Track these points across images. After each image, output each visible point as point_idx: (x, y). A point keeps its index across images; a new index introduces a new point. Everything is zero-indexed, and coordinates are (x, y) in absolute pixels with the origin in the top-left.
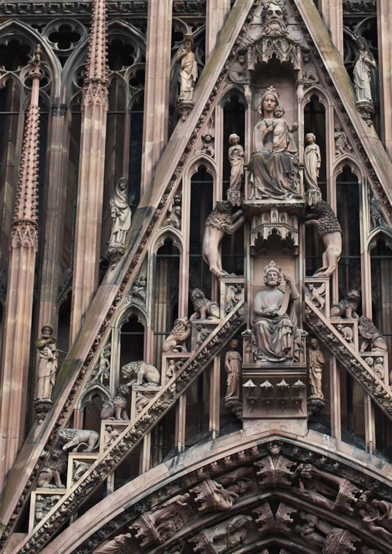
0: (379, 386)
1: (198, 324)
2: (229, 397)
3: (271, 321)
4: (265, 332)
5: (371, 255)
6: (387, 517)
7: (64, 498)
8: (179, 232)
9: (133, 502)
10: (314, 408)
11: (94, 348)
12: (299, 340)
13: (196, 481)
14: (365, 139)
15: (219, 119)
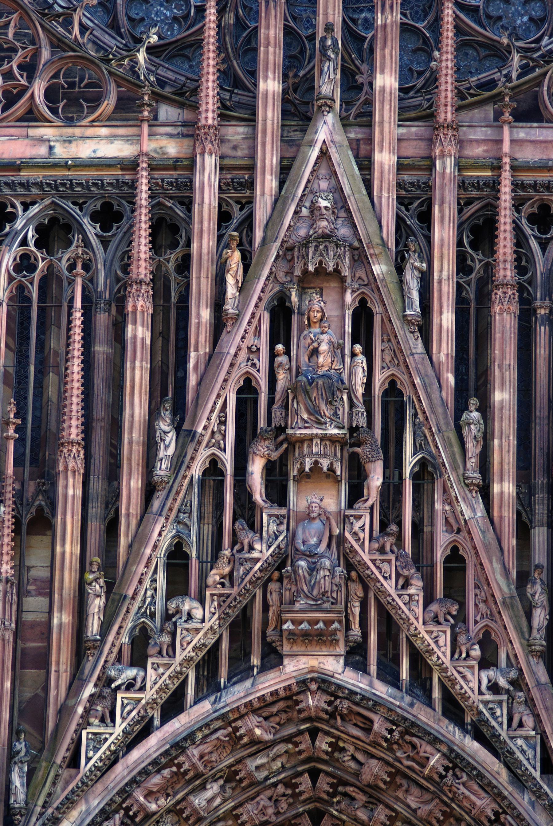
0: (414, 626)
1: (240, 558)
2: (269, 631)
3: (310, 560)
4: (304, 575)
5: (413, 480)
6: (418, 753)
7: (114, 737)
8: (224, 454)
9: (178, 739)
10: (351, 644)
11: (140, 582)
12: (337, 580)
13: (238, 716)
14: (411, 357)
15: (265, 327)
